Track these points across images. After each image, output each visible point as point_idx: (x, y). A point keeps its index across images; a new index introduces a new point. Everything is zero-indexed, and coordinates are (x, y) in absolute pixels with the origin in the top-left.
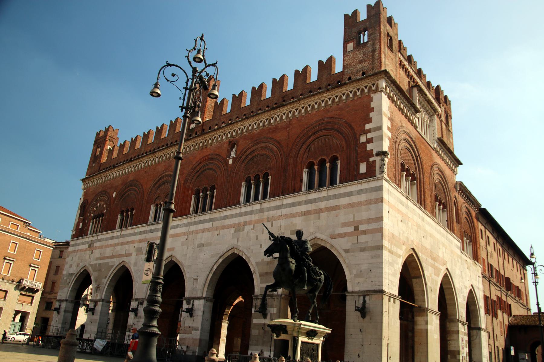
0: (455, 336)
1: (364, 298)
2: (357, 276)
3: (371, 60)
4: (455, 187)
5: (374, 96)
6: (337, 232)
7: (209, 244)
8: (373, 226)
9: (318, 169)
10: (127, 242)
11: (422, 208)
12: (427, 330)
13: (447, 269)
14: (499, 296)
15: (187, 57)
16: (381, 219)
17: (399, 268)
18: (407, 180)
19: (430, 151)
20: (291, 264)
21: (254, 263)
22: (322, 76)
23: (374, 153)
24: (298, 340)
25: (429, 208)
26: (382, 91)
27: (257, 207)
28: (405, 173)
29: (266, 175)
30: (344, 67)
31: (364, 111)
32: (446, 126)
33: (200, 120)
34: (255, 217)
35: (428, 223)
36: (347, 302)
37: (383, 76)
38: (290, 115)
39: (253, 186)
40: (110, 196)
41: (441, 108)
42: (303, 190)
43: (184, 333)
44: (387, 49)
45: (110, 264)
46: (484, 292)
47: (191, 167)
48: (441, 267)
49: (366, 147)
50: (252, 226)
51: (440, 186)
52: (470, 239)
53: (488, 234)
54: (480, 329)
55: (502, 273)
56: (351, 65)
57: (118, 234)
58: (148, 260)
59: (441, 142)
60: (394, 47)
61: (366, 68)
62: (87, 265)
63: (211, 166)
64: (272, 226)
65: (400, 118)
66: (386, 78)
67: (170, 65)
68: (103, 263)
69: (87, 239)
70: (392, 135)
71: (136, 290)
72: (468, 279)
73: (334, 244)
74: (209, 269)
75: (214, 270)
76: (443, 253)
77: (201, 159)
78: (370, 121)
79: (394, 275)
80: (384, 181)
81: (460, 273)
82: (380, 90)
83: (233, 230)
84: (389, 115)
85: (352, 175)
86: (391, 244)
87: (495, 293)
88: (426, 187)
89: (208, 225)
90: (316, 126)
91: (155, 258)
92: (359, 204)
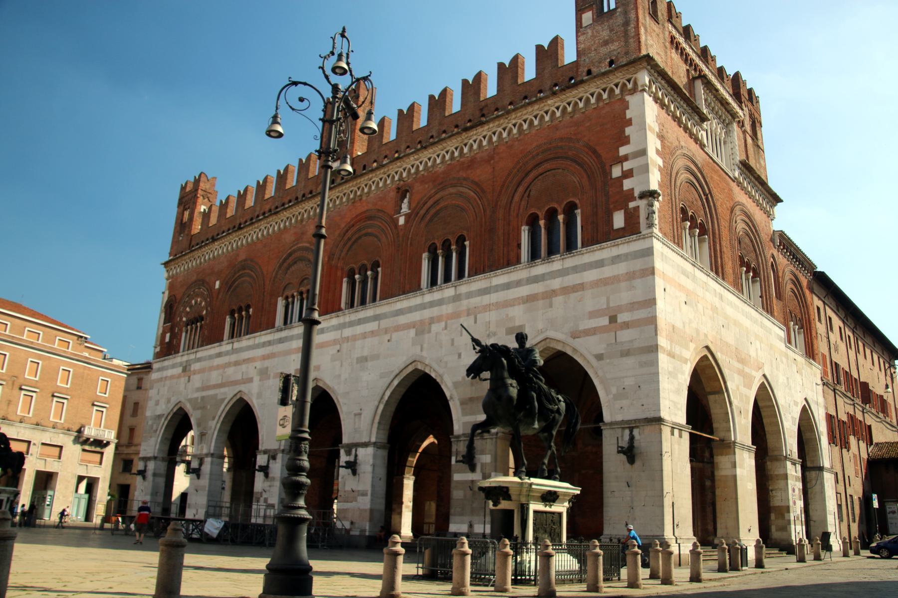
0: (781, 483)
1: (631, 429)
2: (617, 397)
3: (623, 39)
4: (772, 240)
5: (632, 100)
6: (581, 328)
7: (376, 357)
8: (641, 314)
9: (545, 225)
10: (244, 360)
11: (720, 280)
12: (735, 477)
13: (764, 376)
14: (852, 413)
15: (322, 68)
16: (652, 302)
17: (685, 379)
18: (692, 235)
19: (728, 184)
20: (511, 389)
21: (450, 384)
22: (544, 69)
23: (636, 194)
24: (528, 509)
25: (731, 277)
26: (644, 90)
27: (449, 292)
28: (689, 224)
29: (461, 240)
30: (579, 53)
31: (616, 126)
32: (753, 139)
33: (350, 168)
34: (447, 309)
35: (730, 303)
36: (604, 439)
37: (645, 64)
38: (495, 139)
39: (440, 258)
40: (211, 288)
41: (742, 110)
42: (522, 260)
43: (345, 502)
44: (648, 18)
45: (219, 397)
46: (826, 408)
47: (337, 233)
48: (754, 373)
49: (622, 185)
50: (443, 324)
51: (747, 240)
52: (799, 324)
53: (830, 313)
54: (821, 469)
55: (855, 375)
56: (589, 49)
57: (229, 347)
58: (284, 402)
59: (745, 166)
60: (659, 14)
61: (615, 53)
62: (183, 400)
63: (370, 230)
64: (475, 322)
65: (675, 133)
66: (649, 67)
67: (295, 83)
69: (179, 359)
70: (664, 162)
72: (800, 389)
73: (578, 347)
74: (379, 398)
75: (386, 398)
76: (756, 351)
77: (352, 220)
78: (626, 141)
79: (678, 392)
80: (655, 240)
81: (785, 381)
82: (640, 88)
83: (412, 332)
84: (657, 130)
85: (602, 233)
86: (672, 341)
87: (844, 410)
88: (724, 243)
89: (372, 326)
90: (538, 154)
91: (294, 398)
92: (616, 279)
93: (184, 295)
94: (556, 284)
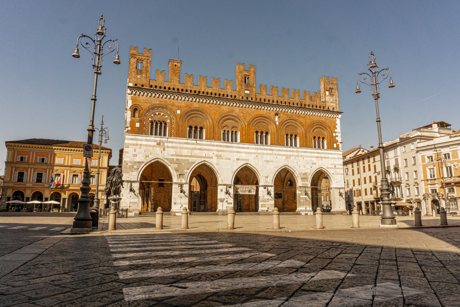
7: (273, 161)
45: (190, 161)
47: (251, 117)
50: (294, 157)
57: (195, 142)
83: (284, 157)
85: (330, 147)
94: (323, 155)
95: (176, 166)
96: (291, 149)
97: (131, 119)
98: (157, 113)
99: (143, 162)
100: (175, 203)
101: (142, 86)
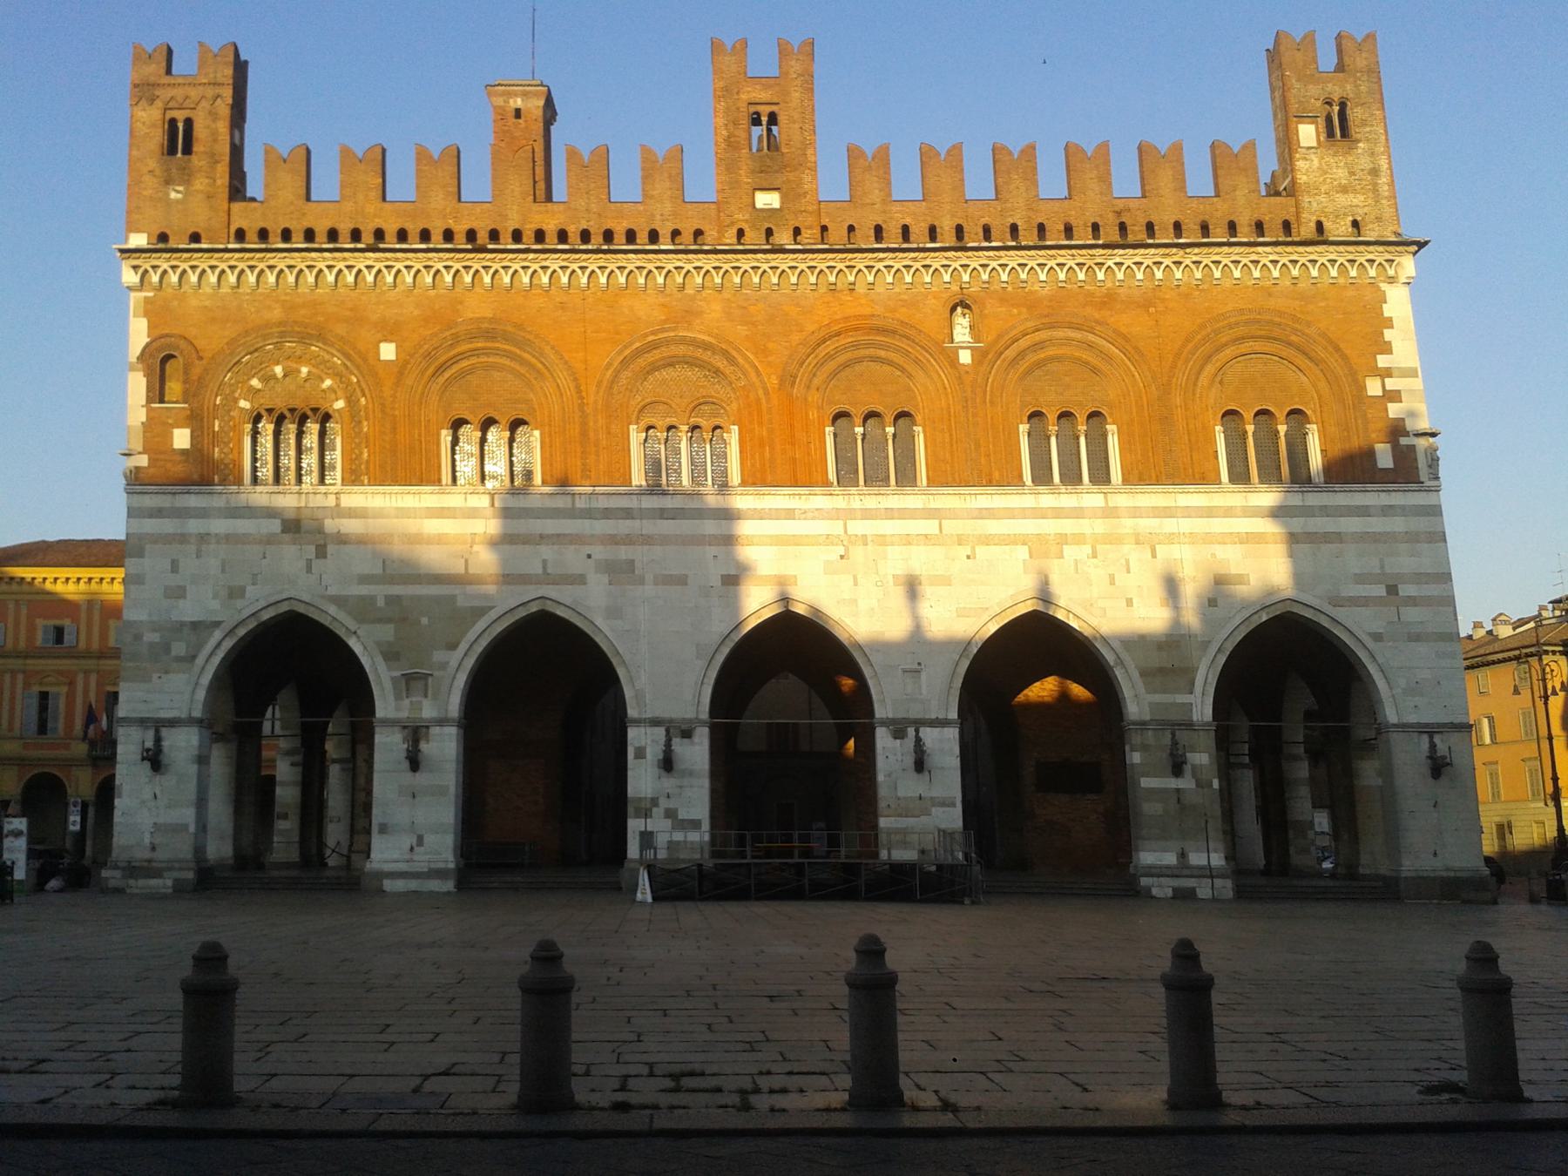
7: (946, 581)
10: (541, 536)
27: (1090, 498)
34: (1085, 526)
45: (461, 602)
68: (419, 598)
71: (639, 696)
83: (1022, 552)
93: (232, 342)
95: (387, 632)
96: (1066, 499)
97: (149, 411)
98: (278, 370)
99: (217, 624)
100: (383, 829)
101: (195, 238)
